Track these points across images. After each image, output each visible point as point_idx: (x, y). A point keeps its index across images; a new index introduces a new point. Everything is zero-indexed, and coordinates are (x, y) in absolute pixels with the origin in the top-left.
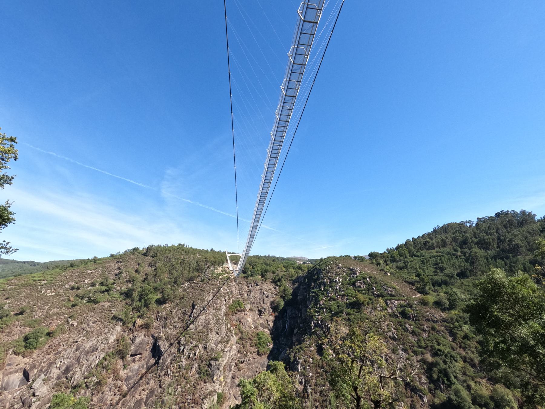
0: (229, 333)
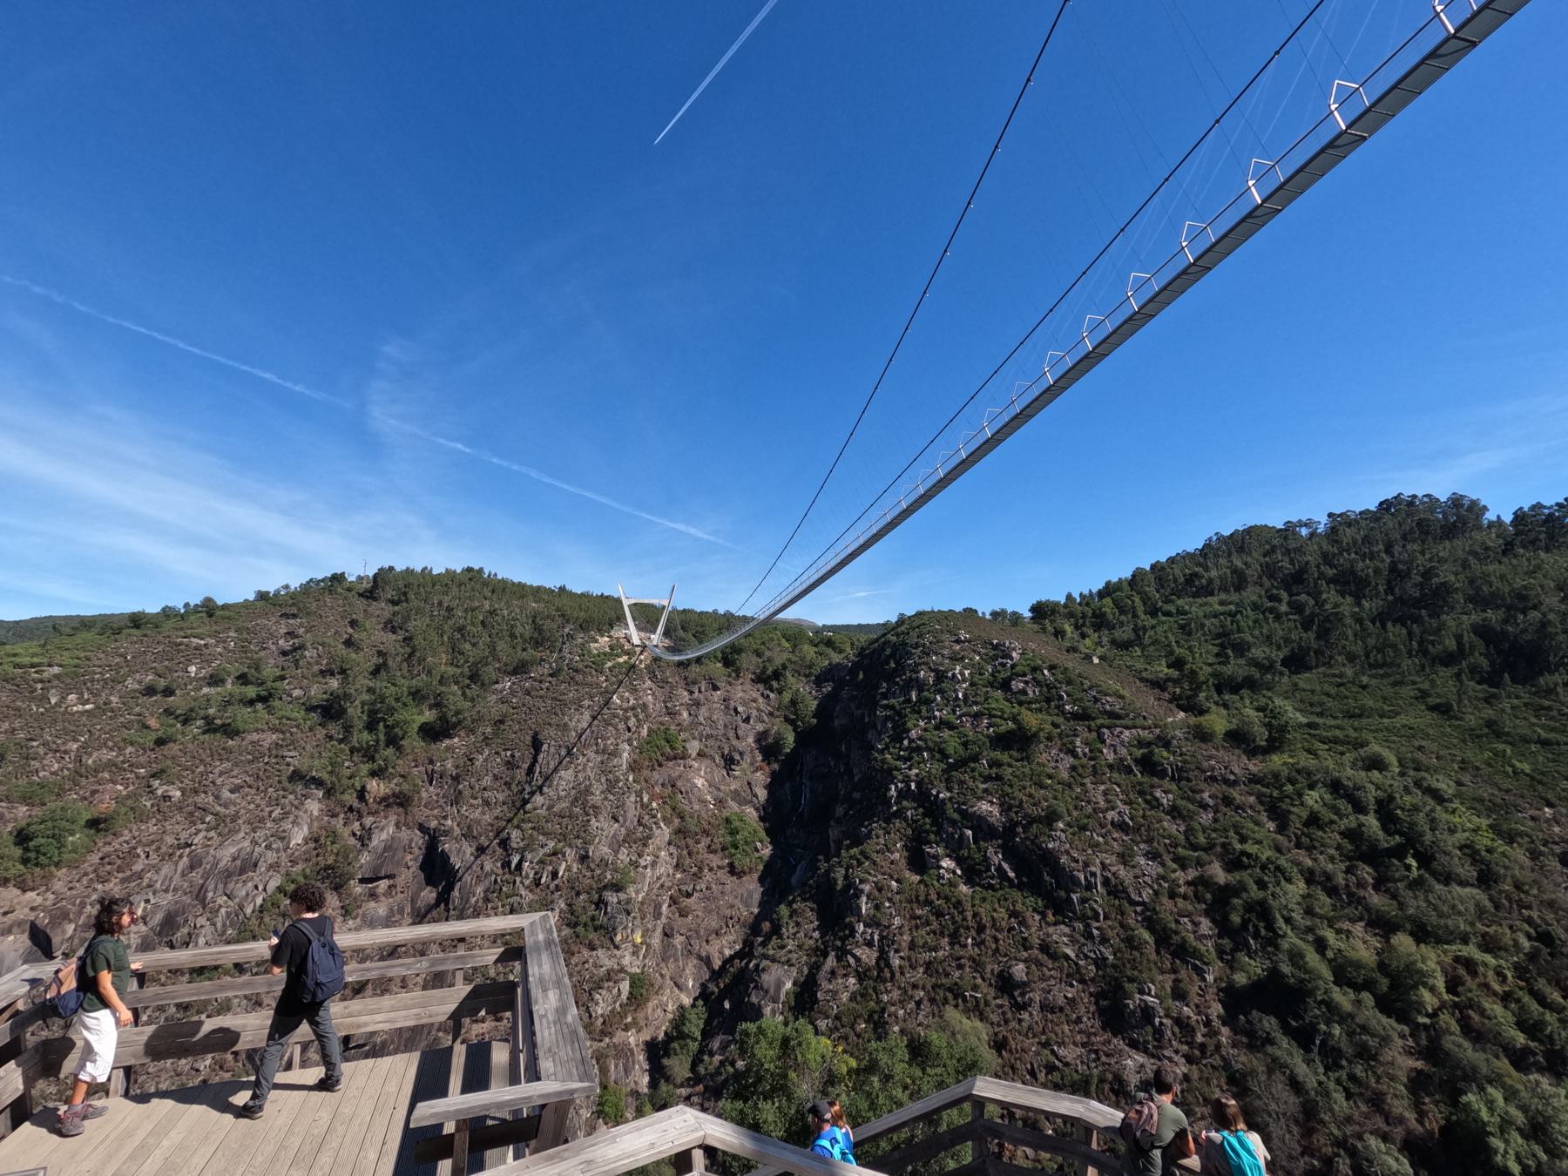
0: (647, 817)
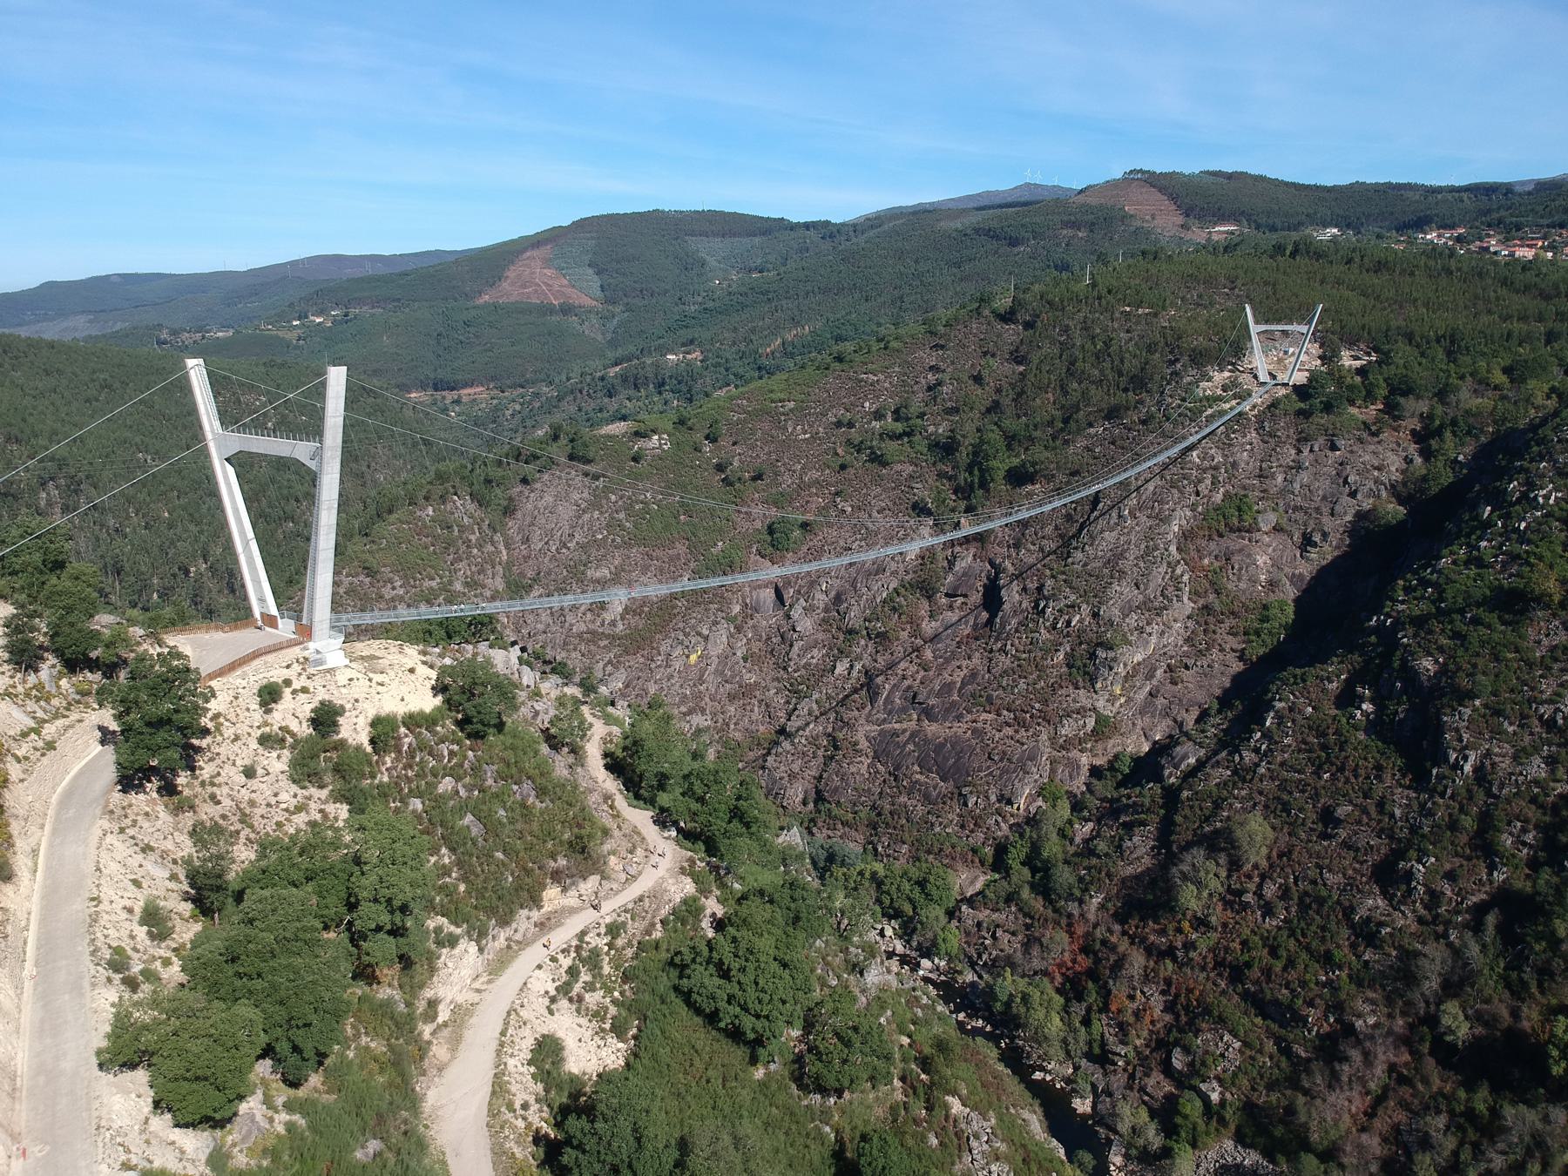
0: (1170, 589)
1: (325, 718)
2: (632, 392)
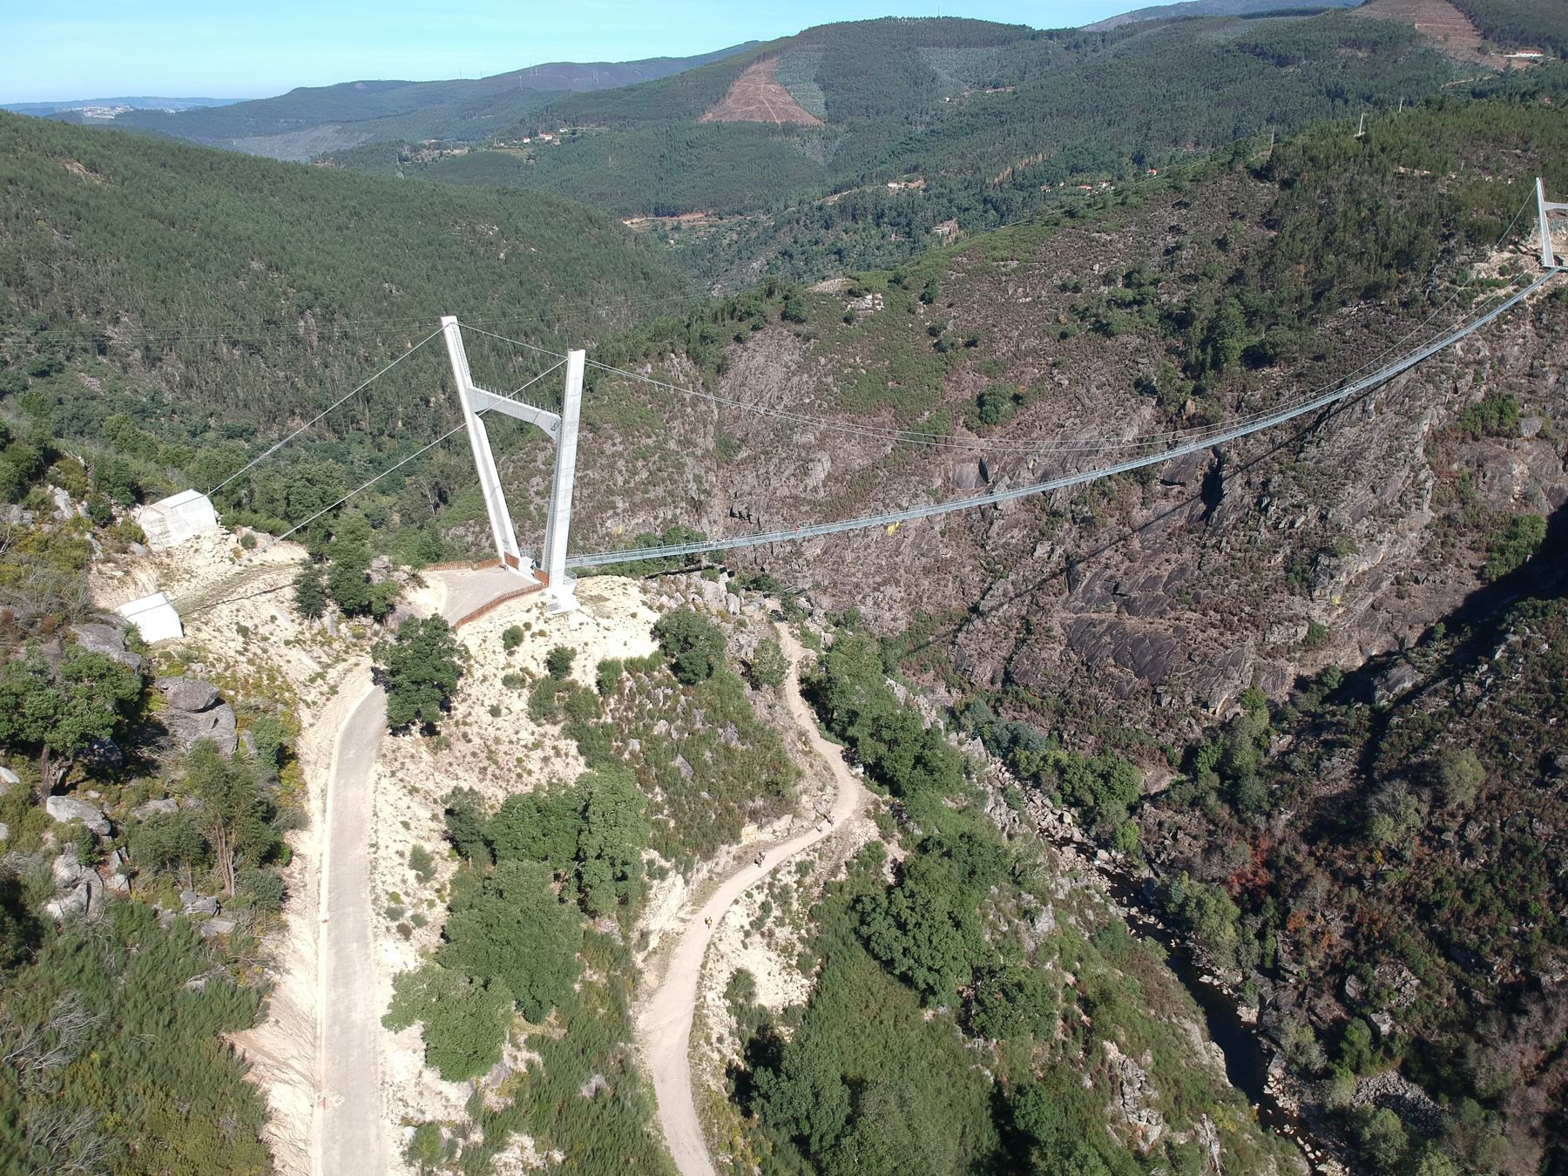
0: (1410, 495)
1: (559, 662)
2: (849, 224)
